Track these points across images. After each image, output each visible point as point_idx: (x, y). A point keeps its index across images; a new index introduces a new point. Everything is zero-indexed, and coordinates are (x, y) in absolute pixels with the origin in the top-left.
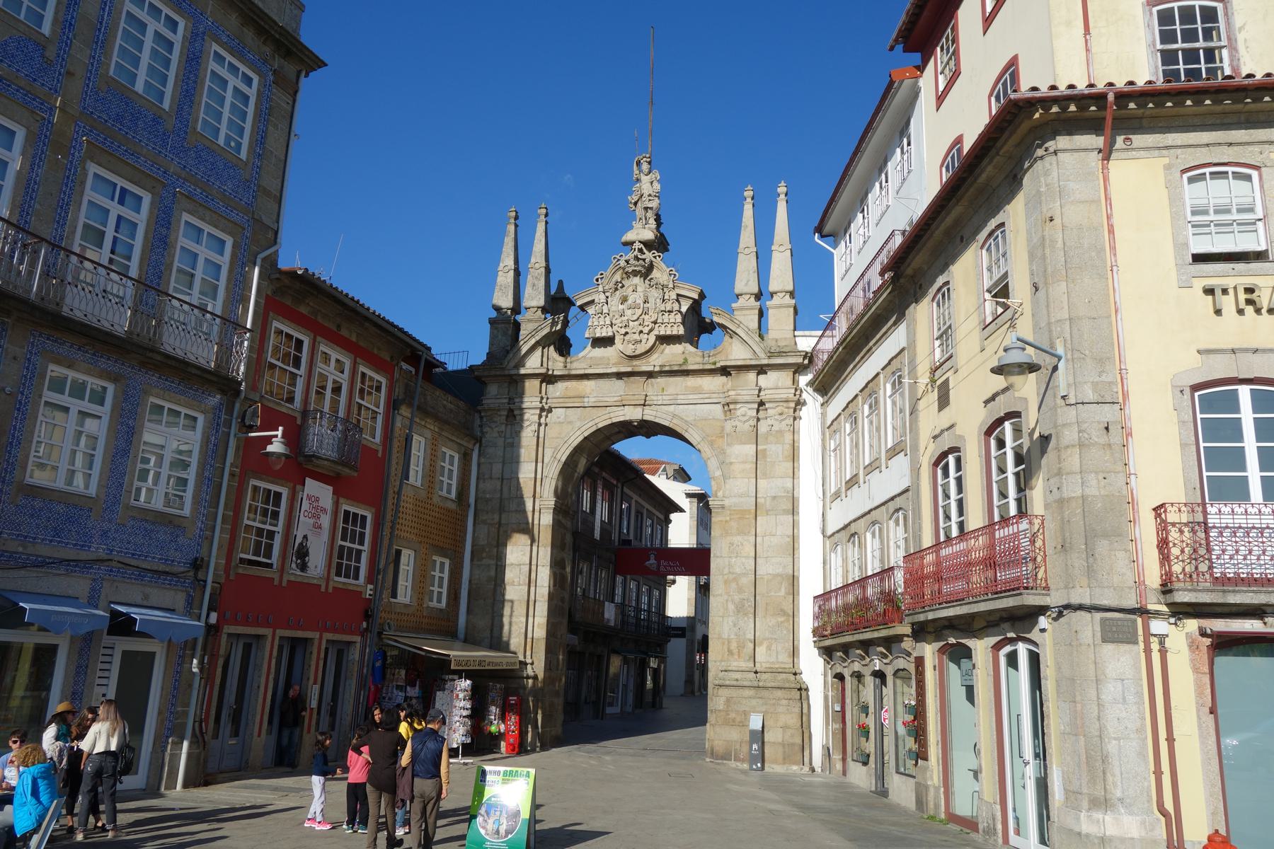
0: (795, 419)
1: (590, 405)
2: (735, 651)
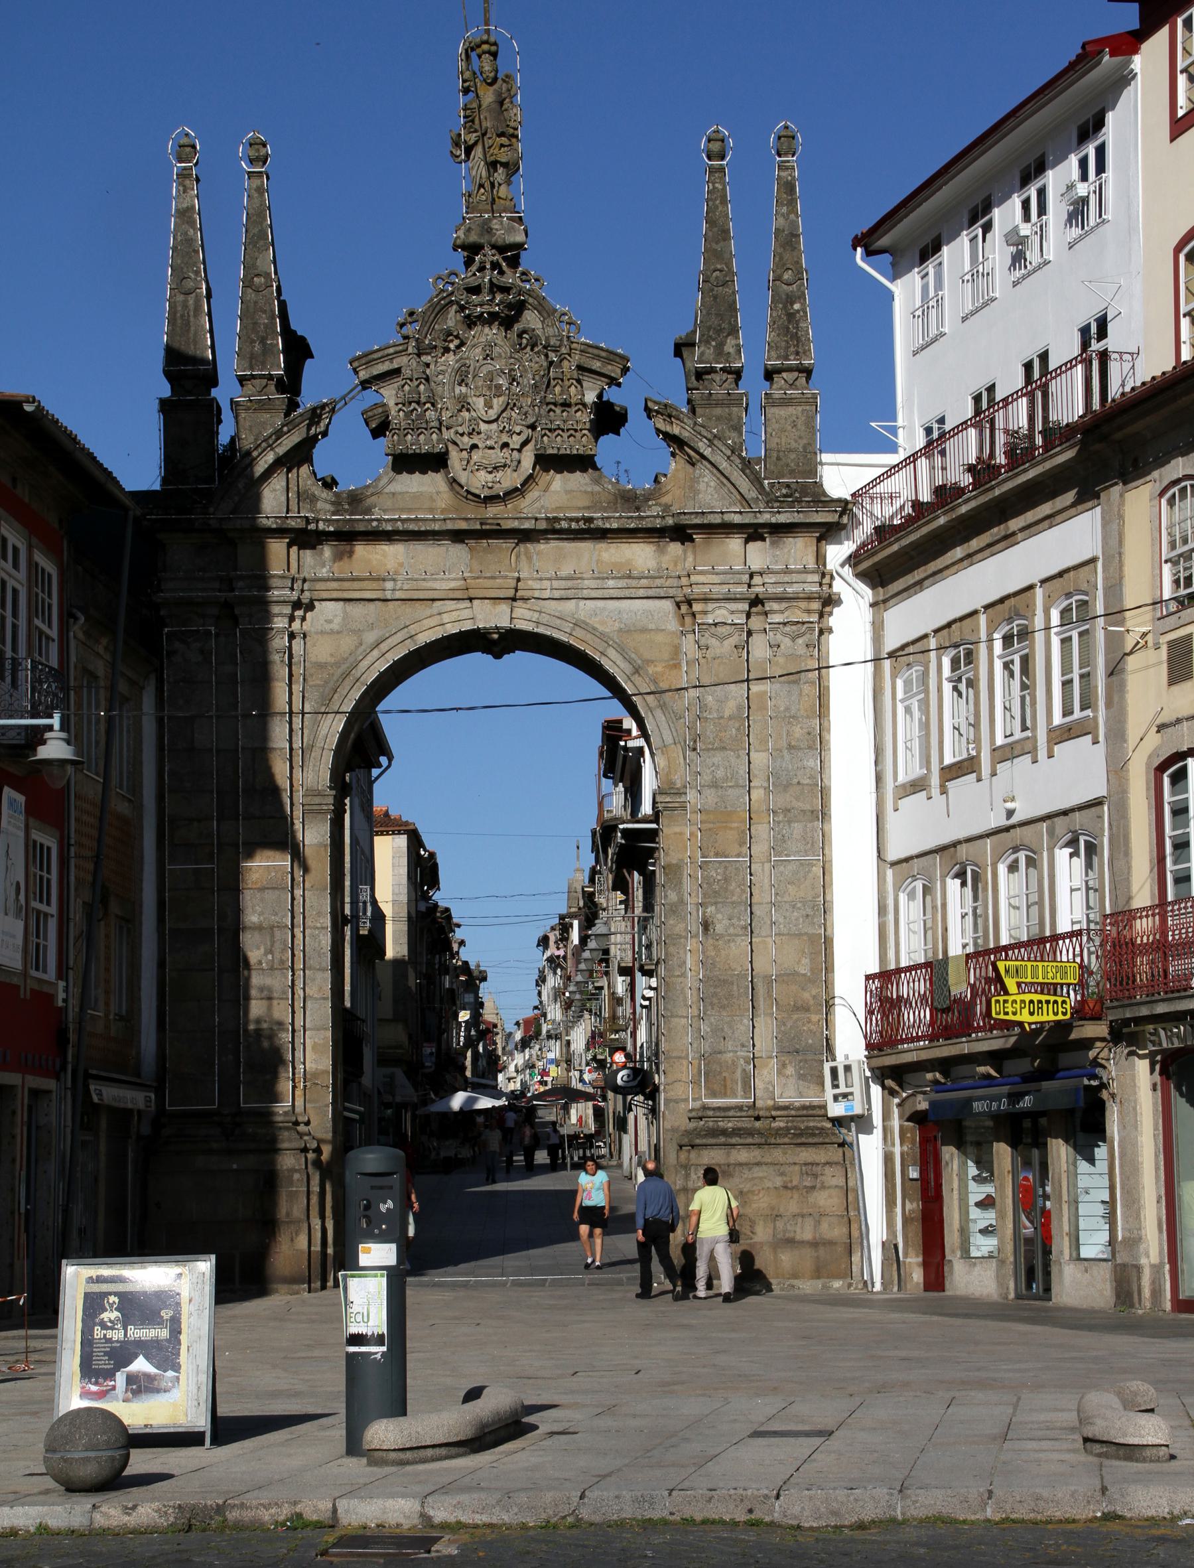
0: (821, 632)
1: (398, 595)
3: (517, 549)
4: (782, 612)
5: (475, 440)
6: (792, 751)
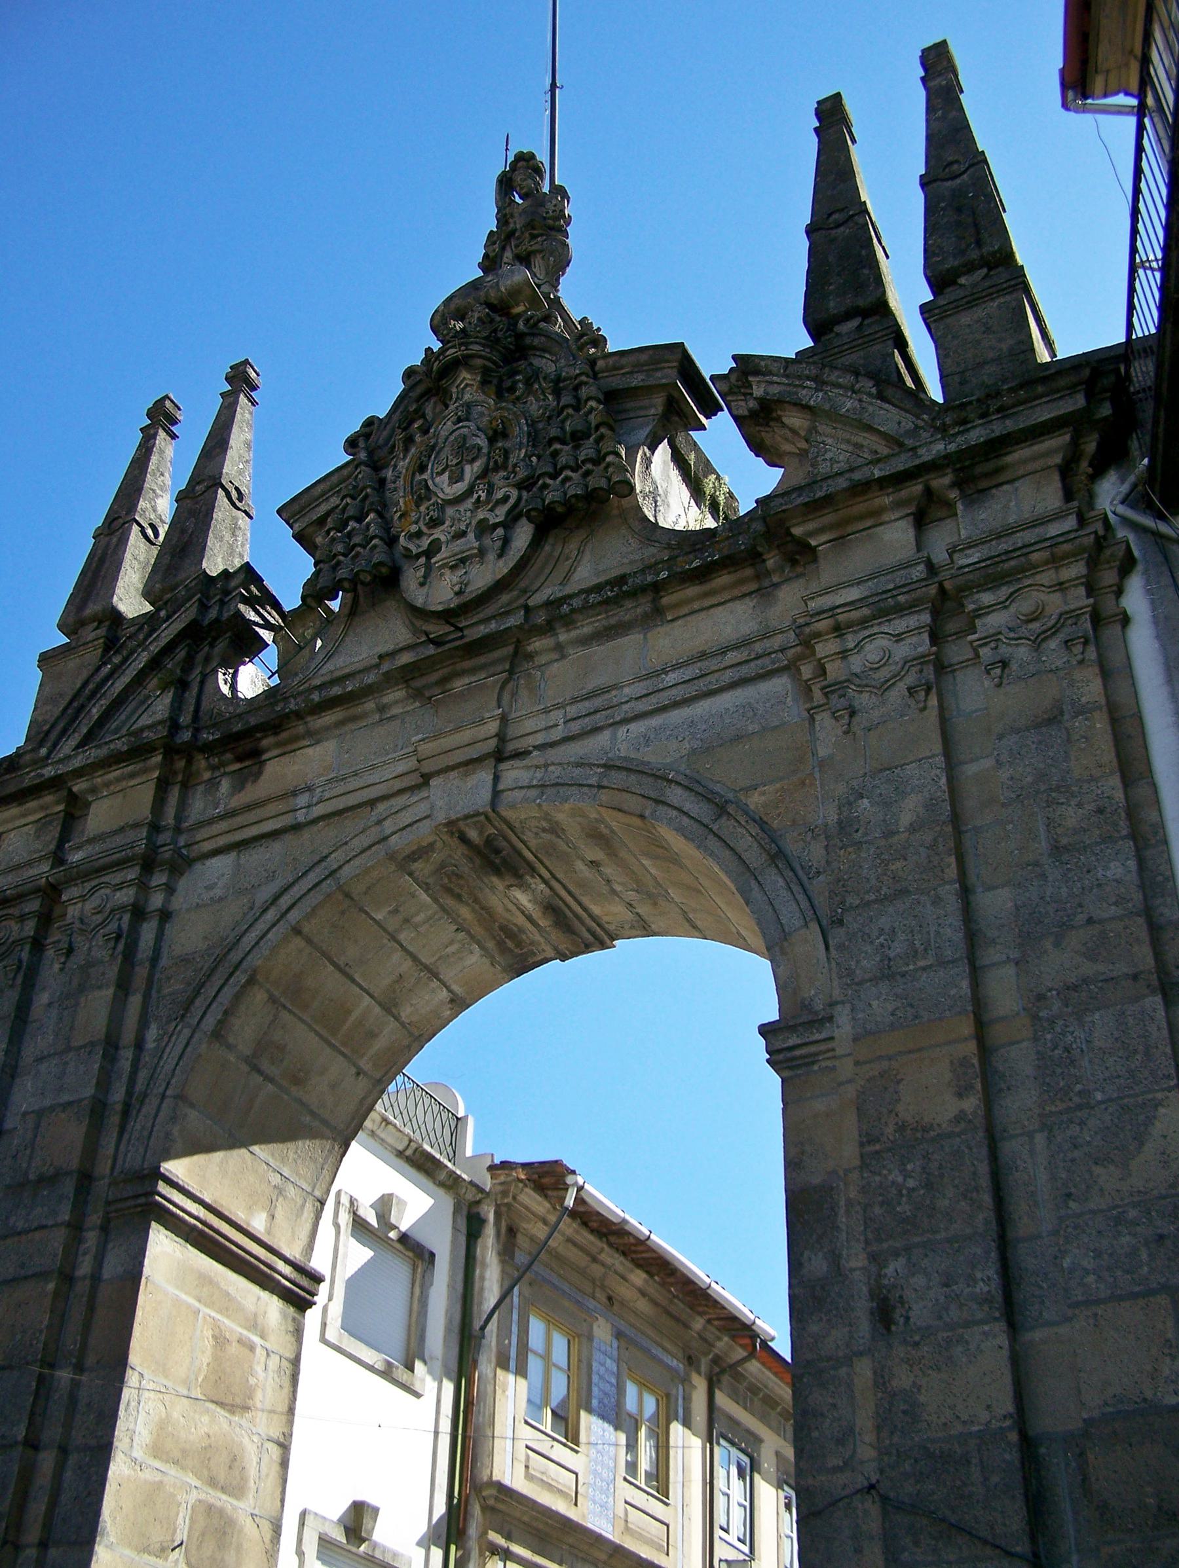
1: (318, 811)
3: (510, 685)
4: (1003, 605)
5: (439, 534)
6: (1065, 857)
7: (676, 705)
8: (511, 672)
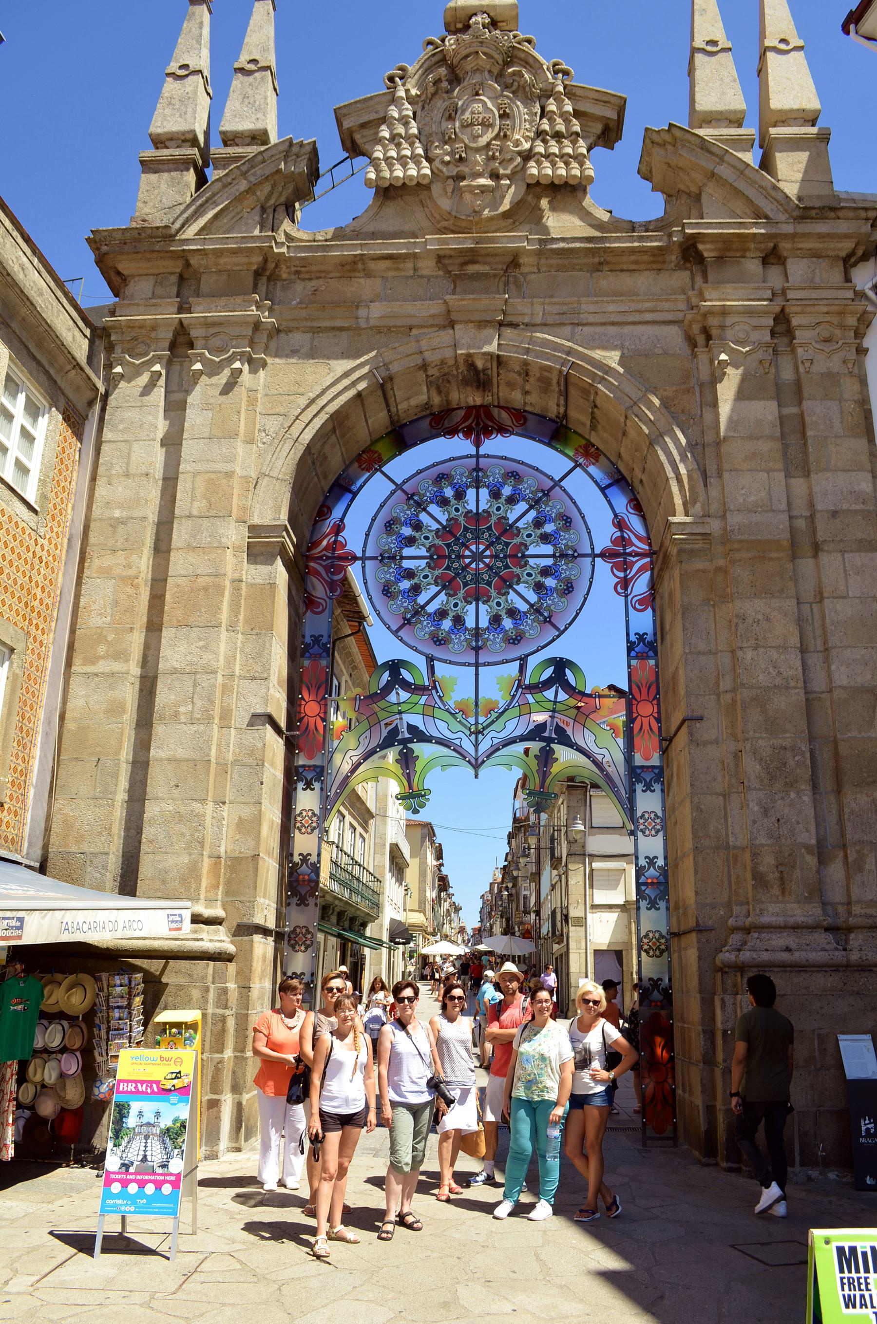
2: (772, 877)
4: (813, 328)
7: (613, 324)
8: (506, 271)
